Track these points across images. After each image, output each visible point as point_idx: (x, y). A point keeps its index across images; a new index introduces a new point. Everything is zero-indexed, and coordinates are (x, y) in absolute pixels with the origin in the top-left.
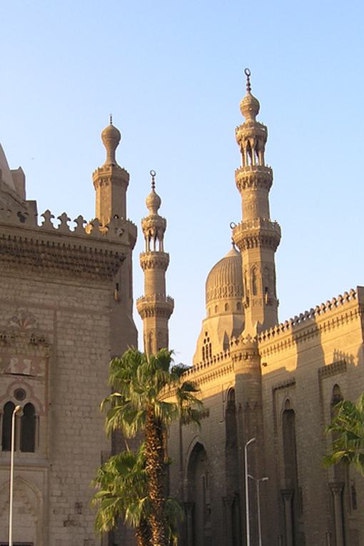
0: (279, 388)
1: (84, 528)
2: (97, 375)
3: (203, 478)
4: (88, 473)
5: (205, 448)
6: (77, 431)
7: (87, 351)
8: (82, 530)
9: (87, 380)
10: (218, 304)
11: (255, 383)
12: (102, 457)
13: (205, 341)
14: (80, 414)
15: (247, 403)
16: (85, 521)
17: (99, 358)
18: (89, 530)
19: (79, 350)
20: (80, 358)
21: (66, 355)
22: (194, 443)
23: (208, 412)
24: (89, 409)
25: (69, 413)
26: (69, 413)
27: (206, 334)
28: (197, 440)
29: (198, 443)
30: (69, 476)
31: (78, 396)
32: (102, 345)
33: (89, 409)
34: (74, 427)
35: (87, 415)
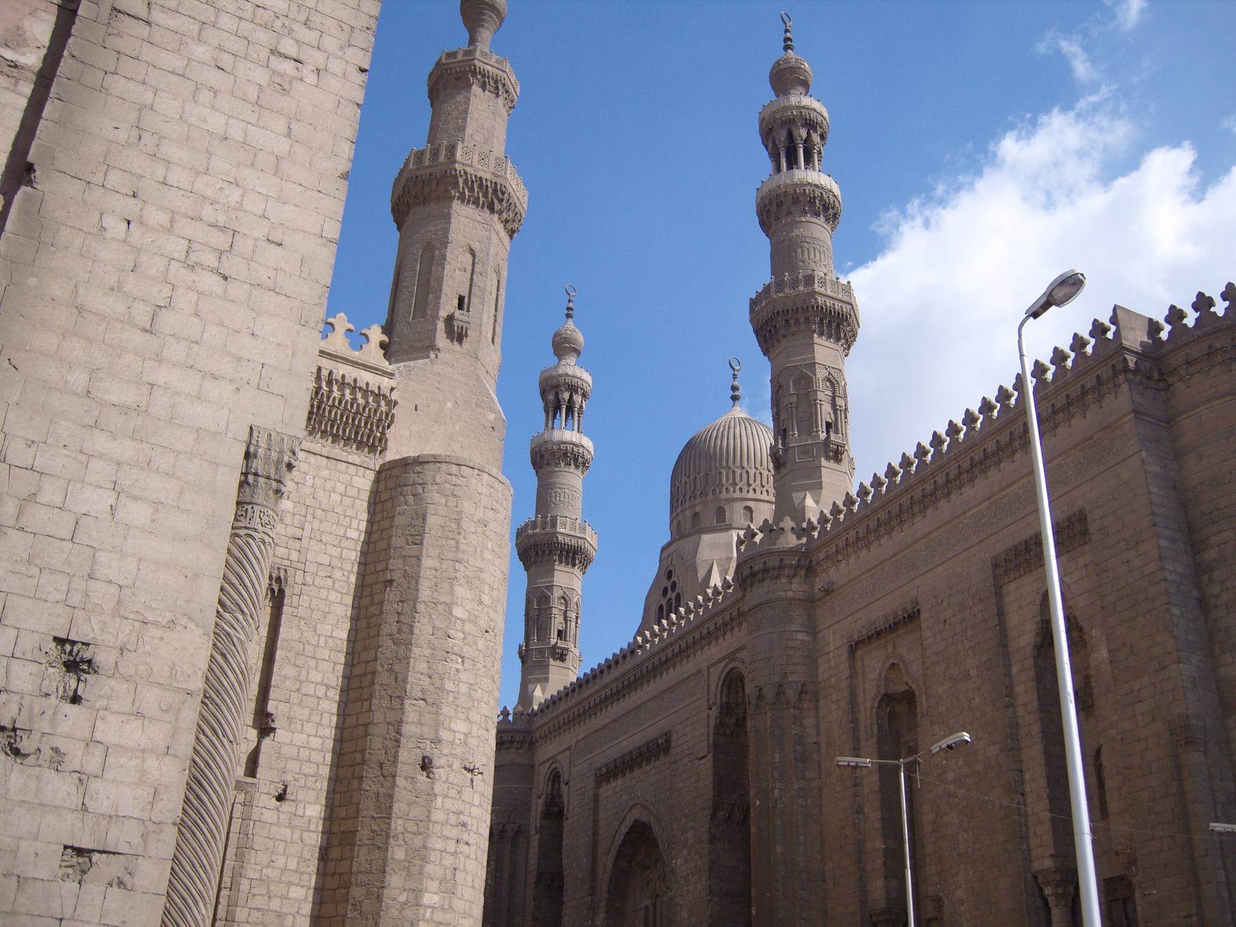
0: (869, 638)
1: (82, 778)
2: (289, 133)
3: (647, 908)
4: (157, 504)
5: (657, 833)
6: (142, 314)
7: (262, 36)
8: (59, 788)
9: (236, 132)
10: (698, 509)
11: (801, 636)
12: (248, 456)
13: (665, 591)
14: (176, 247)
15: (780, 685)
16: (91, 742)
17: (311, 78)
18: (103, 797)
19: (226, 22)
20: (220, 48)
21: (157, 16)
22: (629, 822)
23: (668, 742)
24: (222, 241)
25: (116, 228)
26: (116, 228)
27: (670, 574)
28: (636, 814)
29: (636, 821)
30: (51, 493)
31: (178, 176)
32: (331, 44)
33: (222, 241)
34: (131, 285)
35: (210, 260)
